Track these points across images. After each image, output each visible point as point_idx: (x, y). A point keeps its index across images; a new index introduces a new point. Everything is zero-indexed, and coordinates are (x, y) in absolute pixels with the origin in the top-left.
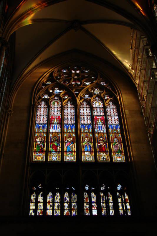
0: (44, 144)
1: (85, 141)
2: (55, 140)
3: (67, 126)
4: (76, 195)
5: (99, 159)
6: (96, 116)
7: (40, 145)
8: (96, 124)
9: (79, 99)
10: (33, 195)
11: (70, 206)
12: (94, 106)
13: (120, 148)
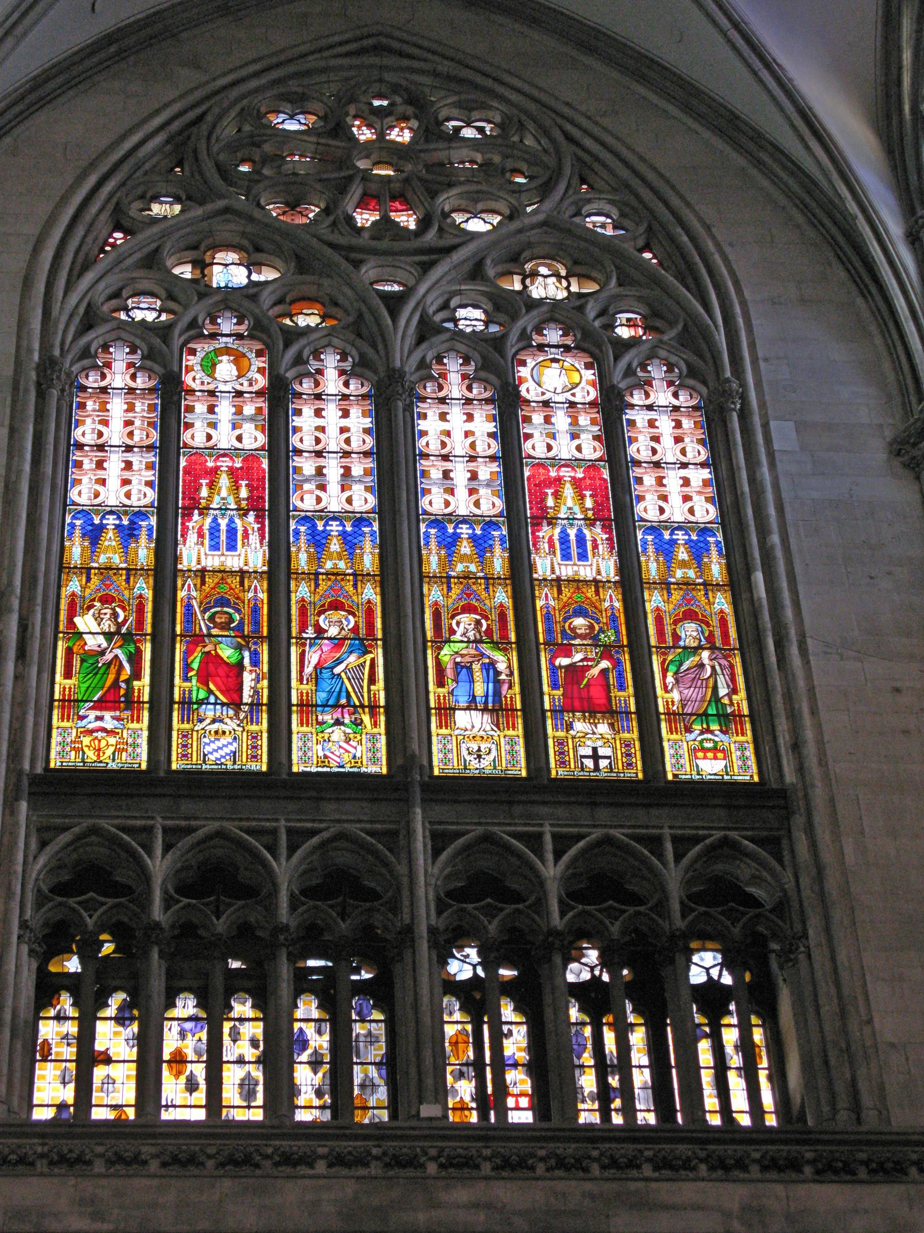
0: (139, 652)
1: (457, 637)
2: (225, 626)
3: (314, 526)
4: (377, 1015)
5: (563, 763)
6: (540, 465)
7: (109, 656)
8: (543, 517)
9: (410, 340)
10: (52, 1013)
12: (530, 390)
13: (723, 691)
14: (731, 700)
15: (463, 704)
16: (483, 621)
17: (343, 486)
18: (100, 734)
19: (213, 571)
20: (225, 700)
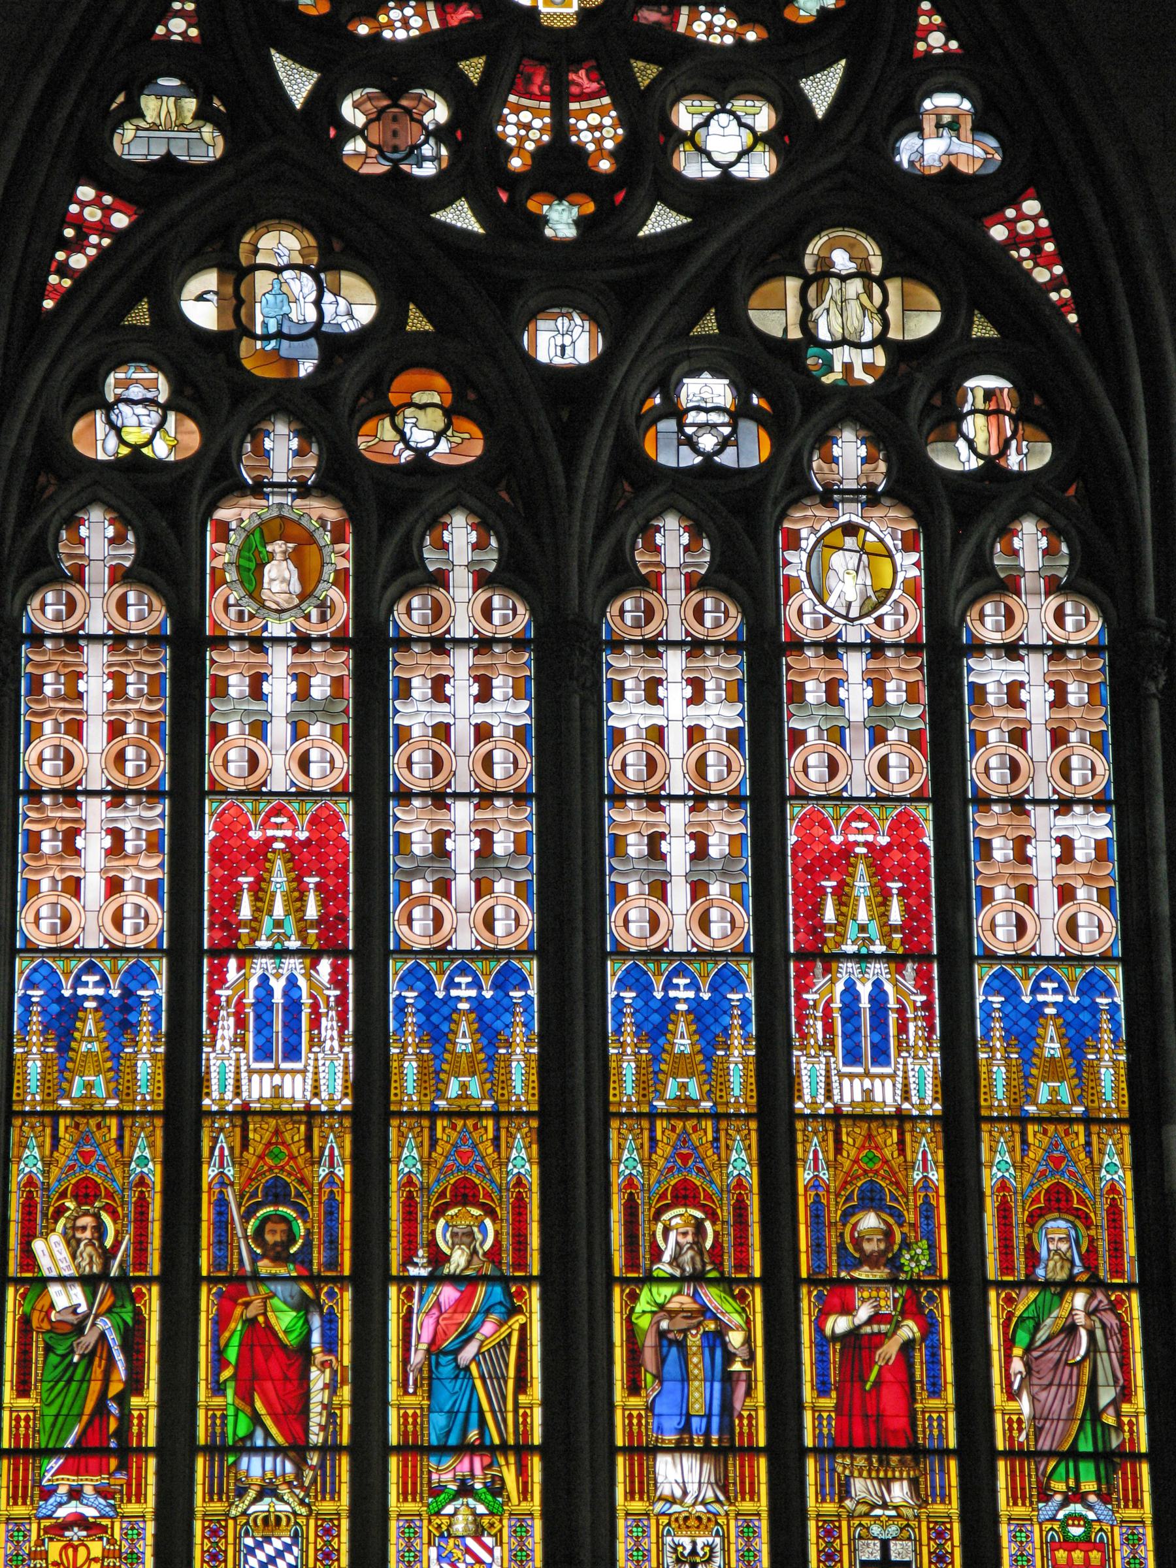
0: (140, 1319)
1: (664, 1268)
2: (279, 1255)
7: (89, 1338)
13: (1106, 1396)
14: (1118, 1415)
15: (670, 1438)
16: (708, 1224)
17: (478, 883)
18: (75, 1534)
19: (263, 1114)
20: (281, 1440)
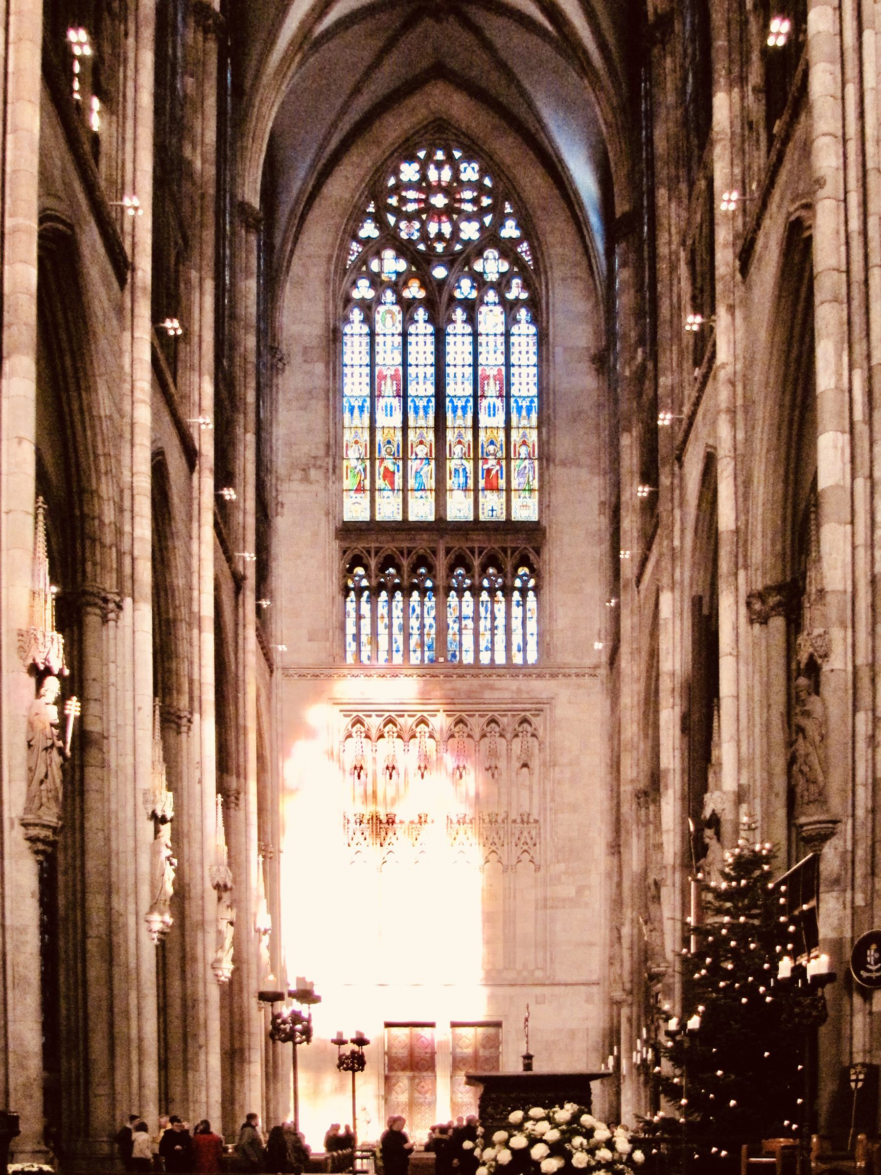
11: (422, 627)
